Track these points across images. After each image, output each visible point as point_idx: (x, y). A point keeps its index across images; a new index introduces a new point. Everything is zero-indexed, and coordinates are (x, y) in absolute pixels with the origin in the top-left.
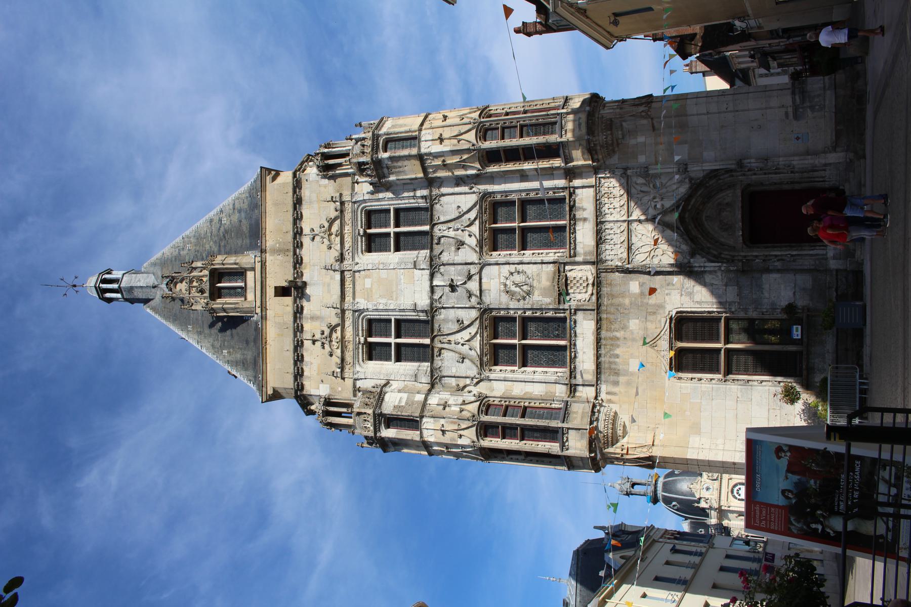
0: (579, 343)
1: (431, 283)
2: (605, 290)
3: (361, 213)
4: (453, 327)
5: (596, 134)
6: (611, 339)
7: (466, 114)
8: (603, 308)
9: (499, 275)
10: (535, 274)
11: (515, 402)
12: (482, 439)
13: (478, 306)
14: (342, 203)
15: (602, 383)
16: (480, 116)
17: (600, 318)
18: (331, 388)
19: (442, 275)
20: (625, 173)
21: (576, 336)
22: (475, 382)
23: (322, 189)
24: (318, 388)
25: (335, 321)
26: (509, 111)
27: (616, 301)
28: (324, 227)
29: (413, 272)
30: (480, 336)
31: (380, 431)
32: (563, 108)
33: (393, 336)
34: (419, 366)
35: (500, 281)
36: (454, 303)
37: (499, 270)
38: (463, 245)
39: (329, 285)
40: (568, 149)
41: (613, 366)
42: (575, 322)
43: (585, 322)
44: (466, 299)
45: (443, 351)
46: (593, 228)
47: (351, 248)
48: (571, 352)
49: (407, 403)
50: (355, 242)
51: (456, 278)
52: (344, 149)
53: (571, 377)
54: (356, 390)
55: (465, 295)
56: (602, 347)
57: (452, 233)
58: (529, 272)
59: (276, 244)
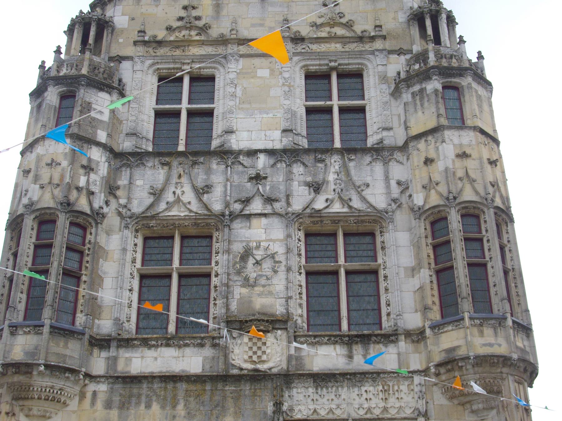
0: (169, 352)
1: (261, 151)
2: (246, 388)
3: (359, 64)
4: (199, 180)
5: (476, 369)
6: (175, 397)
7: (499, 191)
8: (220, 386)
9: (271, 240)
10: (271, 288)
11: (87, 262)
12: (36, 217)
13: (227, 213)
14: (373, 39)
15: (111, 385)
16: (497, 208)
17: (205, 382)
18: (122, 31)
19: (273, 166)
20: (420, 414)
21: (180, 347)
22: (121, 210)
23: (392, 15)
24: (123, 14)
26: (507, 249)
27: (230, 403)
28: (341, 17)
29: (276, 129)
30: (185, 216)
31: (56, 85)
32: (514, 322)
33: (189, 106)
34: (148, 140)
35: (262, 241)
36: (233, 181)
37: (277, 240)
38: (315, 191)
39: (262, 25)
40: (452, 330)
41: (134, 400)
42: (202, 345)
43: (200, 359)
44: (236, 196)
45: (166, 168)
46: (338, 370)
47: (309, 51)
48: (157, 339)
49: (94, 119)
50: (320, 55)
51: (268, 183)
52: (447, 38)
53: (119, 340)
54: (120, 59)
55: (244, 195)
56: (163, 385)
57: (331, 177)
58: (275, 281)
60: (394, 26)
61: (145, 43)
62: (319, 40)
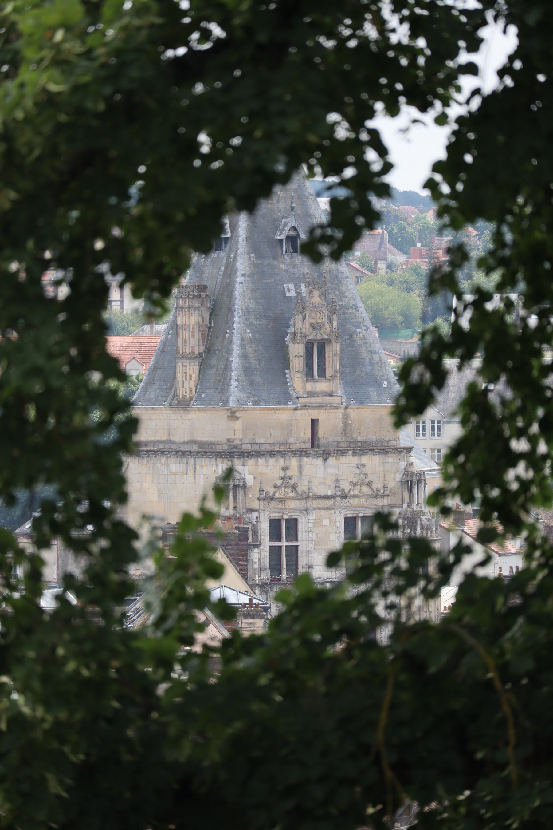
24: (250, 474)
25: (300, 489)
59: (351, 420)
60: (393, 485)
61: (264, 499)
62: (355, 496)
